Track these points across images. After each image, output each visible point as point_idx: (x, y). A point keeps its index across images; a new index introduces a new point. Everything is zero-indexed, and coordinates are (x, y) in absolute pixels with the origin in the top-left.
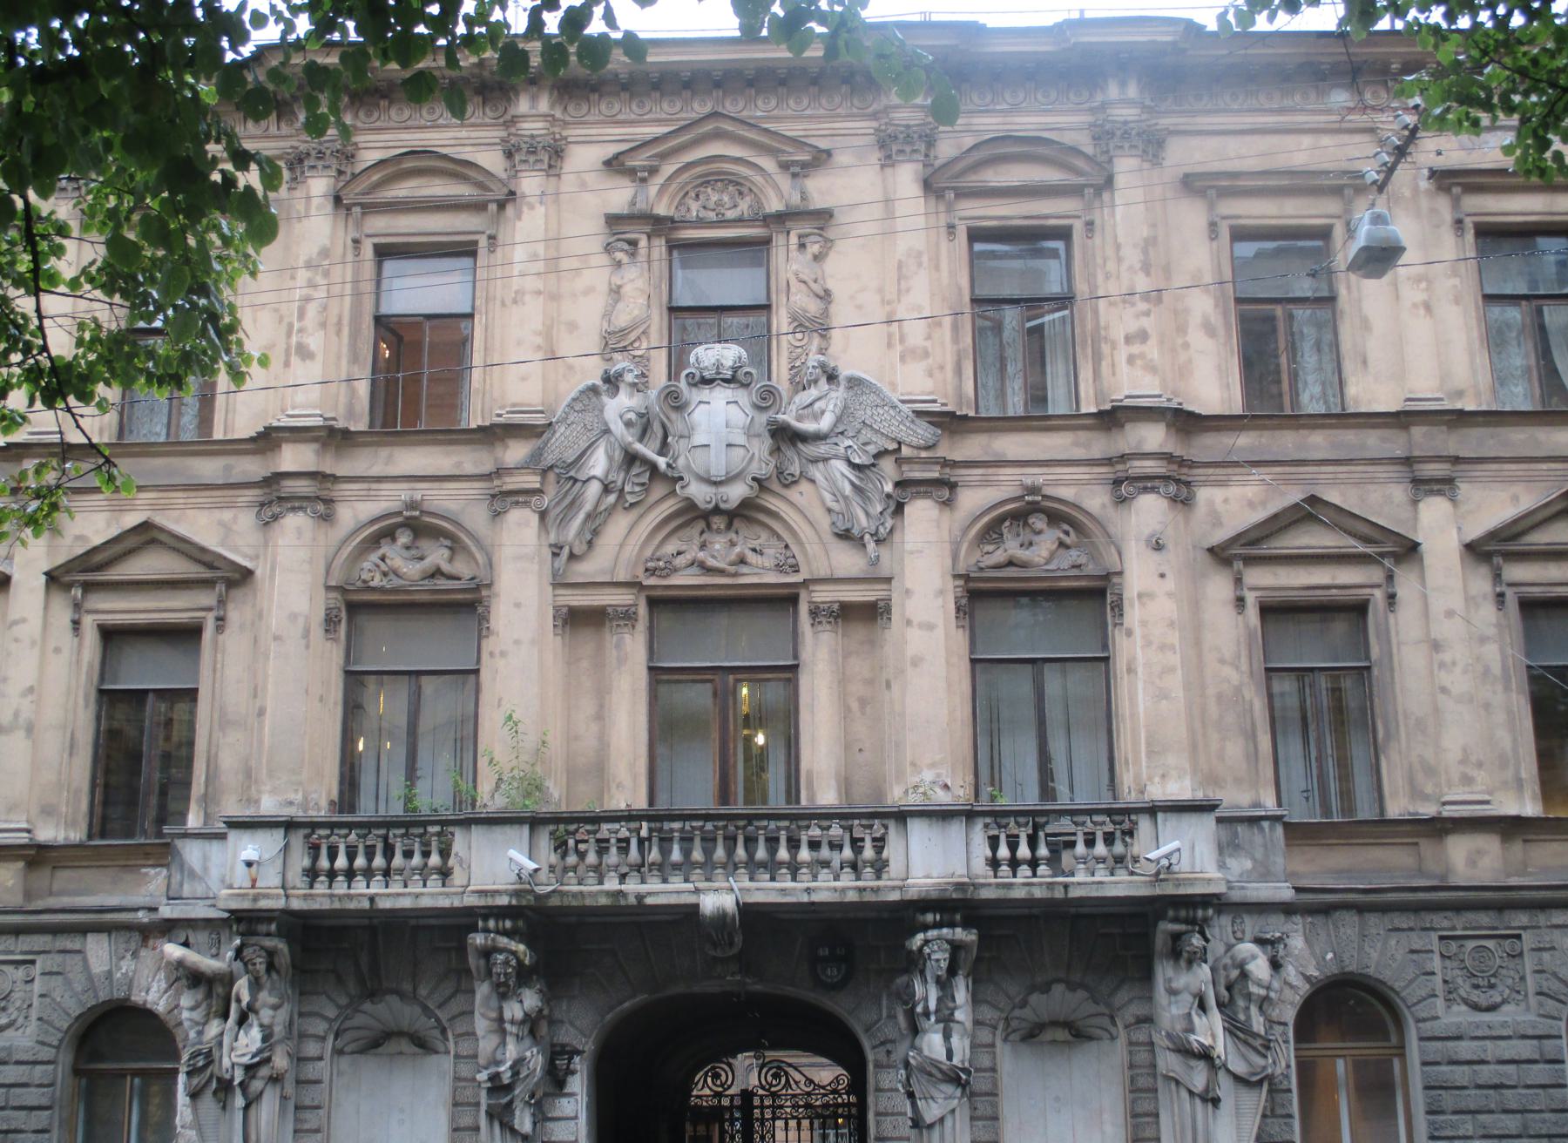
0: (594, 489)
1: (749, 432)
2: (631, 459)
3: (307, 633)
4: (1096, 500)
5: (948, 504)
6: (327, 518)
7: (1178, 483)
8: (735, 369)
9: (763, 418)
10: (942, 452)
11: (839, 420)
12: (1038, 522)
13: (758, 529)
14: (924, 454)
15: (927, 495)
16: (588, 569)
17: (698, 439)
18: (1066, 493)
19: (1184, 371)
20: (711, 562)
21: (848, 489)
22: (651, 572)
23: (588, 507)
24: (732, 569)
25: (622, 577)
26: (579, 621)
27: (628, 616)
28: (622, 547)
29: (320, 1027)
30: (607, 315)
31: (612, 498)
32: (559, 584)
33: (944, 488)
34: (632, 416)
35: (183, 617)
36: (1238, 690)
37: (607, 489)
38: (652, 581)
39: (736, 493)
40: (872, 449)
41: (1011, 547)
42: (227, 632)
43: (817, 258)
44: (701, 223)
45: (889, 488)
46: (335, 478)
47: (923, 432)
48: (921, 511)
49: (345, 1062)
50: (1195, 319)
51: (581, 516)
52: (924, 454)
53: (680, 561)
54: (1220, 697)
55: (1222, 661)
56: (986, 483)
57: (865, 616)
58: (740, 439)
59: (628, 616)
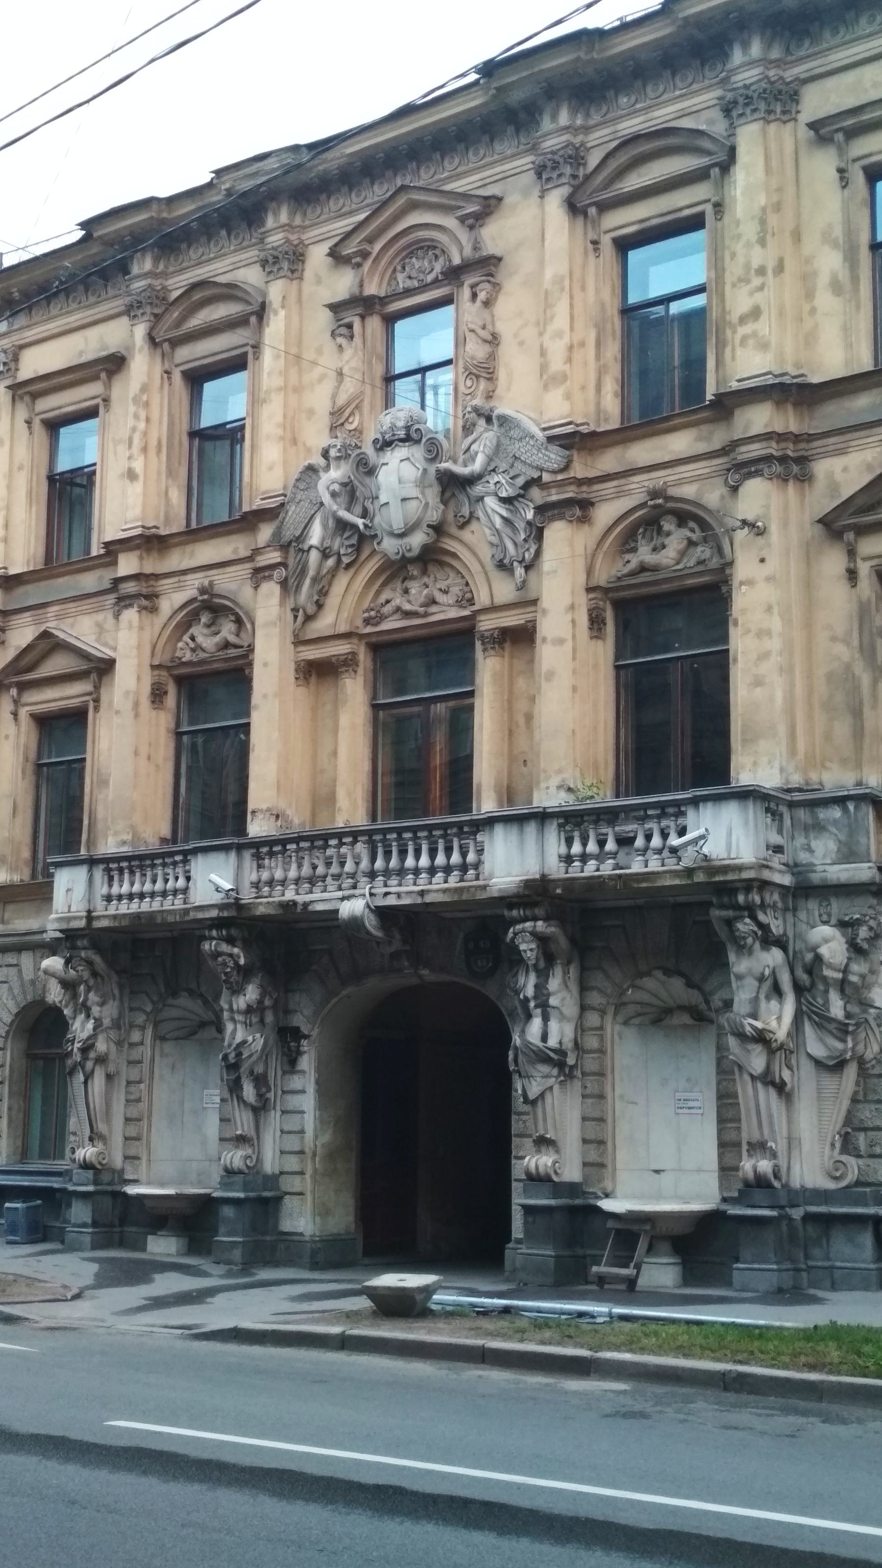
0: (314, 557)
1: (421, 483)
2: (342, 526)
3: (136, 705)
4: (712, 496)
5: (585, 519)
6: (153, 610)
7: (791, 462)
8: (408, 428)
9: (432, 470)
10: (579, 470)
11: (490, 460)
12: (668, 525)
13: (447, 569)
14: (560, 477)
15: (561, 517)
16: (324, 624)
17: (383, 499)
18: (688, 491)
19: (810, 339)
20: (407, 607)
21: (498, 522)
22: (367, 622)
23: (311, 573)
24: (422, 610)
25: (343, 628)
26: (318, 672)
27: (349, 662)
28: (345, 605)
29: (141, 1019)
30: (334, 397)
31: (331, 562)
32: (299, 642)
33: (579, 509)
34: (336, 487)
35: (75, 702)
36: (848, 667)
37: (325, 554)
38: (369, 630)
39: (418, 540)
40: (520, 481)
41: (644, 554)
42: (102, 710)
43: (487, 304)
44: (408, 292)
45: (530, 515)
46: (157, 577)
47: (554, 456)
48: (558, 534)
49: (168, 1047)
50: (824, 279)
51: (307, 582)
52: (560, 477)
53: (387, 609)
54: (830, 677)
55: (834, 639)
56: (620, 494)
57: (521, 638)
58: (414, 492)
59: (349, 662)
